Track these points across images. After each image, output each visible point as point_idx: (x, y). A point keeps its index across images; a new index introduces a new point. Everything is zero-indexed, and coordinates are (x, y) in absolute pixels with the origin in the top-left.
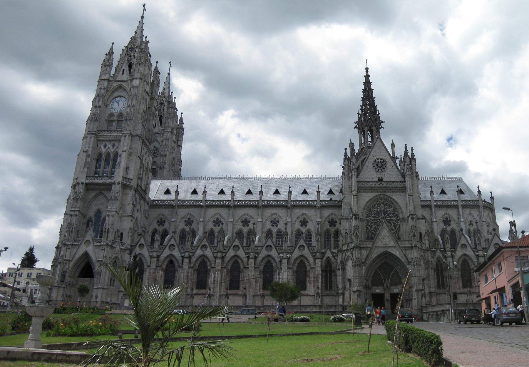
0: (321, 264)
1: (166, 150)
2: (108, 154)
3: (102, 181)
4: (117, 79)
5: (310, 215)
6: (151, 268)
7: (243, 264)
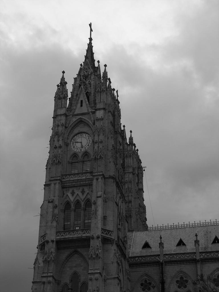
1: (130, 195)
2: (78, 203)
3: (76, 236)
4: (75, 113)
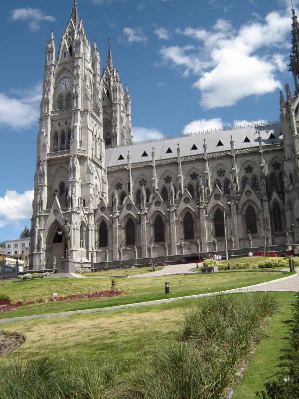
0: (269, 207)
5: (253, 161)
6: (113, 227)
7: (195, 215)
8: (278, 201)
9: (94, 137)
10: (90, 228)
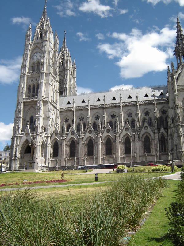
0: (159, 137)
5: (150, 109)
7: (113, 140)
8: (163, 133)
9: (53, 89)
10: (48, 145)
